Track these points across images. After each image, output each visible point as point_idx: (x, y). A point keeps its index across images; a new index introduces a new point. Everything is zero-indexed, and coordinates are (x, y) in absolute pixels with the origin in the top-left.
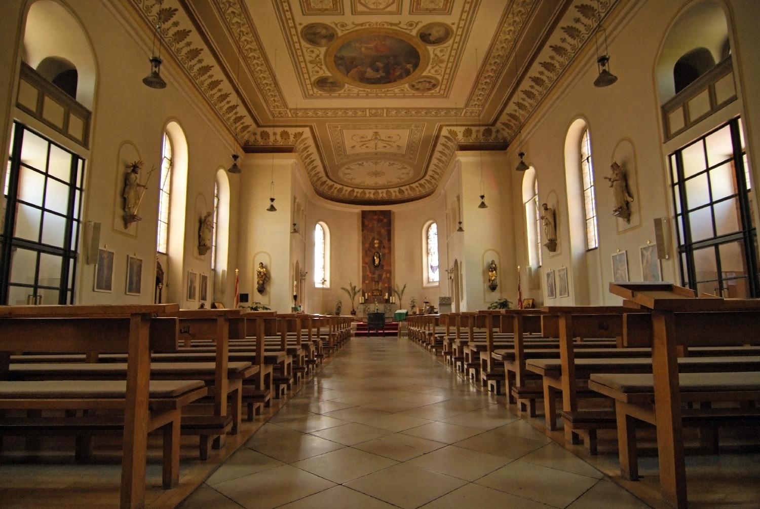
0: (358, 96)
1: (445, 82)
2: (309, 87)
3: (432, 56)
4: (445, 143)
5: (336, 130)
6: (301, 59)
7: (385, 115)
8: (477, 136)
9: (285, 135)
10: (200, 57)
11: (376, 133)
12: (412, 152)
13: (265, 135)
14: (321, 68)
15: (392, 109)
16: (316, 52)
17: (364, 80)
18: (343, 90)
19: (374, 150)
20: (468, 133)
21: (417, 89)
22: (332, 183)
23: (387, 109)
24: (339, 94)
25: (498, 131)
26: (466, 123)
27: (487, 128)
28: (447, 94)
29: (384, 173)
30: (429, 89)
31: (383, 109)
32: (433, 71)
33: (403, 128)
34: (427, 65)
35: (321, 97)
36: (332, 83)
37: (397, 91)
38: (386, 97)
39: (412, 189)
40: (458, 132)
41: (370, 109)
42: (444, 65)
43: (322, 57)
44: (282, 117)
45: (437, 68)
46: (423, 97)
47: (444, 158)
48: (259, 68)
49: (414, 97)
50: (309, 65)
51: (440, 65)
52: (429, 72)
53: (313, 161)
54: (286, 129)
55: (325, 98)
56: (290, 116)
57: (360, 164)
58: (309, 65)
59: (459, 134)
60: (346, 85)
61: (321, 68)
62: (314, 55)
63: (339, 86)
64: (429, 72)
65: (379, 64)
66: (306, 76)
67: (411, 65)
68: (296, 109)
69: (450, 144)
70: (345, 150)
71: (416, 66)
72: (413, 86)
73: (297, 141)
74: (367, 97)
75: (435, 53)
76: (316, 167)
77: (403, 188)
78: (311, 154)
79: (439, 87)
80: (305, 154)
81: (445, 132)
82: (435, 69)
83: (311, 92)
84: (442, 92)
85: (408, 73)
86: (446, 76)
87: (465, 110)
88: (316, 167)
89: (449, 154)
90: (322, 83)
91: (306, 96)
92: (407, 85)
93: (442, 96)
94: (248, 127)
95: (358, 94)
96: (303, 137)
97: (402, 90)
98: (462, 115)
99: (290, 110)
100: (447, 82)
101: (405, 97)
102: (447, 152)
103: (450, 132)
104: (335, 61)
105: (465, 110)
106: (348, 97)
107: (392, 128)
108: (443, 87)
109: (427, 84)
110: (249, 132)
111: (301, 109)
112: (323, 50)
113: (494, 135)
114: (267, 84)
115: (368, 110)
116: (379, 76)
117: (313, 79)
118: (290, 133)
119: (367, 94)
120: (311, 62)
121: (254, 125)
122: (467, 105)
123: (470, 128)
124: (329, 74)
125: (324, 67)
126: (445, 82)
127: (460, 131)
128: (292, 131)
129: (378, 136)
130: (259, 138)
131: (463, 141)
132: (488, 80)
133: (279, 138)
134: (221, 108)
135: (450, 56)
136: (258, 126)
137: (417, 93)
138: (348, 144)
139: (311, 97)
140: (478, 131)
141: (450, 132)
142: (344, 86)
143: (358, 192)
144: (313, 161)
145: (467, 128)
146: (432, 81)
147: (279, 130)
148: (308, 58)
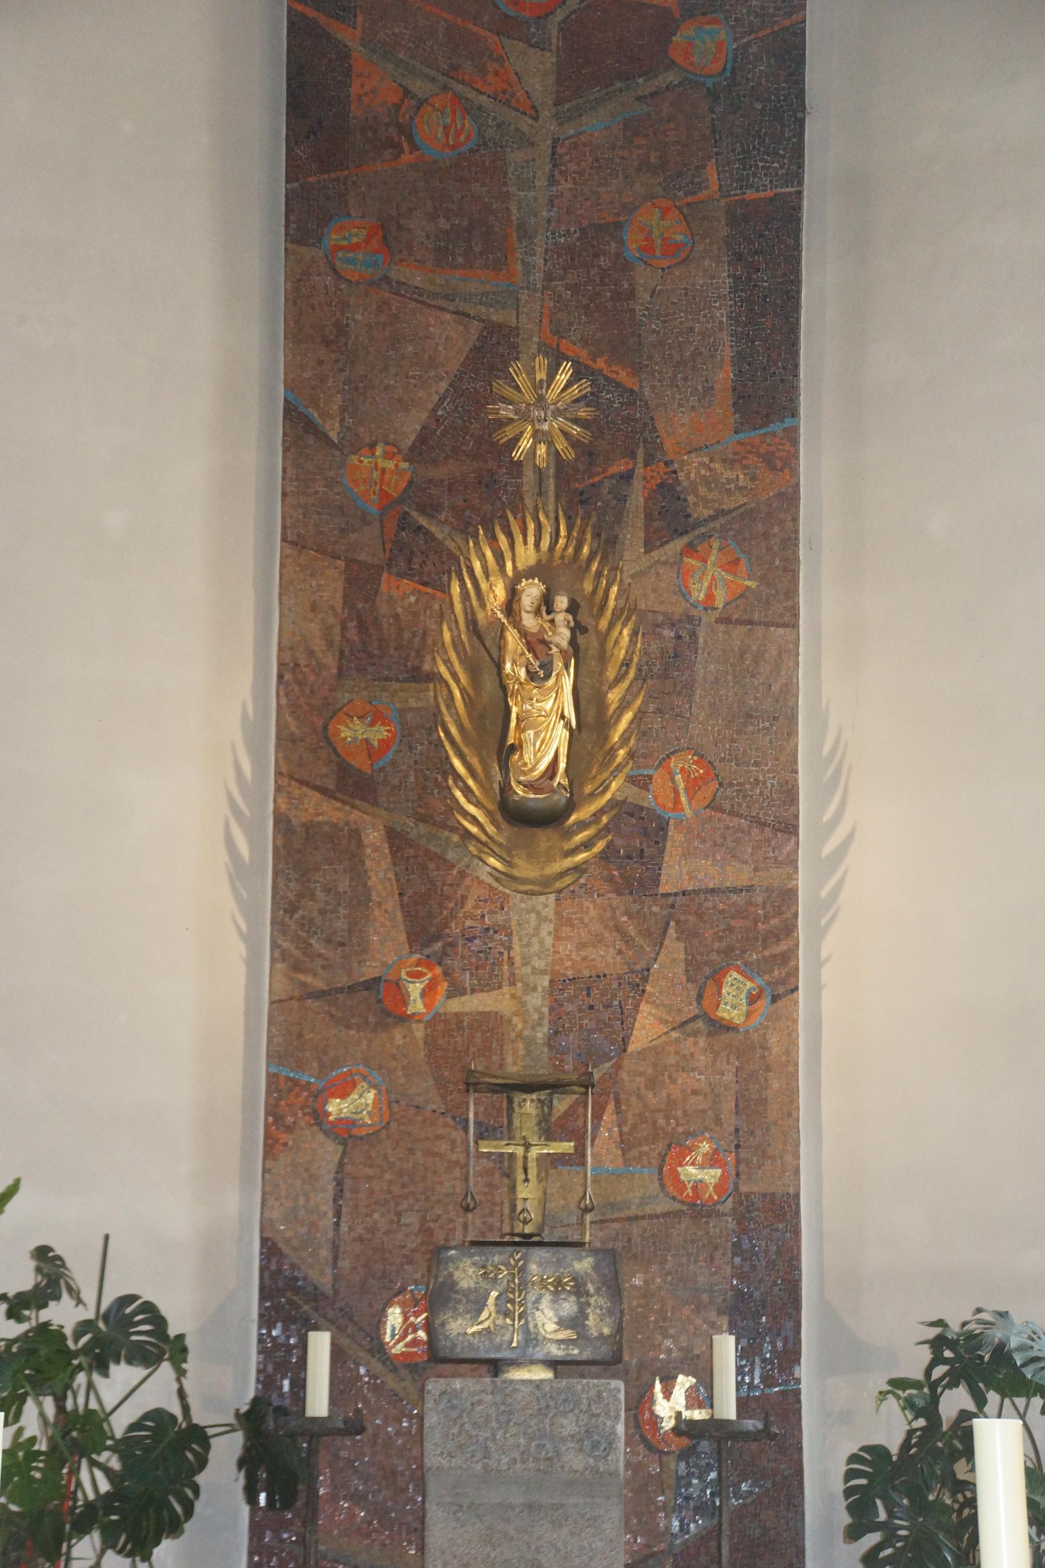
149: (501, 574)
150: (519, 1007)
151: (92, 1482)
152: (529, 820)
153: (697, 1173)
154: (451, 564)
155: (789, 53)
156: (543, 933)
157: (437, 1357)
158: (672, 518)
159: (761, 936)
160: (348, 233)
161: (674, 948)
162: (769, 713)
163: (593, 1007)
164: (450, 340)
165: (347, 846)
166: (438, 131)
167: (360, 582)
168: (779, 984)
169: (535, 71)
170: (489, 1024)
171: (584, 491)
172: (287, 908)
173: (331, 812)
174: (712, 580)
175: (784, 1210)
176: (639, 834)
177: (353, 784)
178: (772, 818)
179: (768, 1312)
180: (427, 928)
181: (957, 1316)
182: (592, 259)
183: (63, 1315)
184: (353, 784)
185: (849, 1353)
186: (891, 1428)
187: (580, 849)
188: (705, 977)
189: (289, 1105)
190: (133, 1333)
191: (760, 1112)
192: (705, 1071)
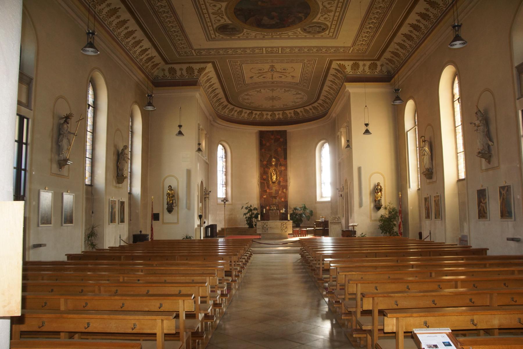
0: (255, 38)
1: (333, 27)
2: (212, 32)
3: (321, 7)
4: (335, 74)
5: (236, 65)
6: (205, 11)
7: (280, 52)
8: (364, 70)
9: (190, 70)
10: (118, 14)
11: (272, 67)
12: (305, 81)
13: (172, 71)
14: (222, 18)
15: (286, 47)
16: (219, 6)
17: (260, 25)
18: (242, 34)
19: (271, 80)
21: (309, 32)
22: (233, 107)
23: (282, 48)
24: (239, 37)
25: (382, 65)
26: (354, 58)
27: (372, 62)
28: (336, 35)
29: (280, 99)
30: (319, 32)
31: (278, 48)
32: (322, 18)
33: (296, 62)
34: (317, 14)
35: (222, 39)
36: (232, 29)
37: (290, 34)
38: (281, 38)
39: (306, 111)
41: (266, 48)
42: (332, 14)
43: (223, 9)
44: (187, 56)
45: (326, 16)
46: (314, 38)
47: (334, 86)
48: (168, 19)
49: (306, 38)
50: (211, 15)
51: (329, 14)
52: (319, 18)
53: (216, 89)
54: (191, 65)
55: (227, 40)
56: (195, 54)
57: (258, 91)
58: (212, 17)
59: (347, 67)
60: (245, 30)
61: (222, 18)
62: (216, 8)
63: (237, 31)
64: (319, 19)
65: (274, 14)
66: (209, 24)
67: (303, 14)
68: (200, 49)
69: (339, 75)
70: (244, 80)
71: (307, 15)
72: (305, 30)
73: (200, 74)
74: (263, 38)
75: (324, 4)
76: (218, 94)
77: (298, 110)
78: (213, 84)
79: (328, 30)
80: (208, 84)
81: (334, 65)
82: (324, 16)
83: (213, 36)
84: (331, 34)
85: (300, 20)
86: (334, 23)
87: (352, 48)
88: (218, 94)
89: (339, 84)
90: (224, 29)
91: (209, 38)
92: (299, 29)
93: (331, 38)
94: (157, 64)
95: (255, 37)
96: (206, 71)
97: (295, 33)
98: (350, 52)
99: (195, 50)
100: (336, 27)
101: (297, 38)
102: (337, 81)
103: (339, 65)
104: (235, 13)
105: (352, 48)
106: (247, 39)
107: (287, 63)
108: (332, 30)
109: (318, 29)
110: (158, 69)
111: (204, 50)
112: (224, 4)
113: (379, 68)
114: (175, 31)
115: (264, 49)
116: (274, 23)
117: (215, 26)
119: (264, 37)
120: (213, 13)
121: (163, 63)
122: (354, 43)
123: (357, 62)
124: (230, 22)
125: (225, 17)
126: (333, 27)
127: (348, 65)
128: (196, 67)
129: (274, 69)
130: (167, 73)
131: (351, 73)
132: (371, 26)
133: (185, 73)
134: (135, 52)
135: (337, 7)
136: (166, 63)
137: (308, 36)
138: (247, 76)
139: (213, 39)
140: (364, 65)
142: (243, 31)
143: (256, 114)
144: (216, 89)
145: (354, 62)
146: (322, 26)
147: (185, 66)
148: (211, 11)
149: (272, 170)
150: (273, 191)
151: (253, 216)
152: (274, 183)
153: (283, 200)
154: (269, 169)
155: (286, 140)
156: (274, 188)
157: (270, 210)
158: (281, 165)
159: (286, 187)
160: (263, 150)
161: (281, 188)
162: (286, 175)
163: (277, 192)
164: (269, 156)
165: (264, 183)
166: (268, 144)
167: (264, 169)
168: (287, 190)
169: (273, 141)
171: (276, 165)
172: (261, 186)
174: (283, 168)
175: (287, 201)
176: (279, 183)
178: (286, 181)
179: (286, 207)
180: (268, 187)
183: (252, 208)
184: (264, 180)
185: (290, 208)
186: (292, 212)
187: (276, 184)
188: (283, 189)
189: (261, 197)
190: (255, 209)
191: (286, 196)
192: (283, 194)
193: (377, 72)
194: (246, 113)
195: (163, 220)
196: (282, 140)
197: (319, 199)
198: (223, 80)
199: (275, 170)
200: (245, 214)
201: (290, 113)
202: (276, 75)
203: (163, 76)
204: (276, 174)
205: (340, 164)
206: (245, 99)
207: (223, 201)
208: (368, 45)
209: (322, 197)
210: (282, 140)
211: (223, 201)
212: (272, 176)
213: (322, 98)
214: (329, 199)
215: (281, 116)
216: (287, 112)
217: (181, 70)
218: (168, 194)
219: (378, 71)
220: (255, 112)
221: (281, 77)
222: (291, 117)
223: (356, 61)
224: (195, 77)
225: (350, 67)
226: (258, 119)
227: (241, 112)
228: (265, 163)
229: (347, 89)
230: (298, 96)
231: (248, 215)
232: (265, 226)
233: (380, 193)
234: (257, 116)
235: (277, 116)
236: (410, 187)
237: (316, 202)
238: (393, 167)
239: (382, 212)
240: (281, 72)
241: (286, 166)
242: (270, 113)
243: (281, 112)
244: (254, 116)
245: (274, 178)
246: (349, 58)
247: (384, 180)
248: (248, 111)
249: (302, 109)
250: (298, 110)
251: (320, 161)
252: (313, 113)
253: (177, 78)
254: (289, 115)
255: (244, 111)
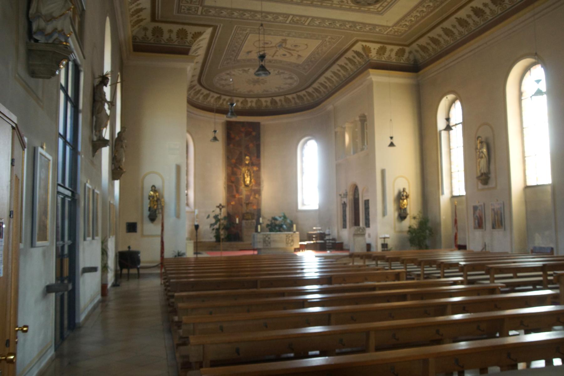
9: (182, 34)
13: (158, 32)
20: (381, 51)
25: (410, 52)
27: (401, 47)
40: (372, 49)
54: (186, 27)
73: (195, 41)
81: (358, 47)
103: (364, 48)
113: (406, 55)
118: (188, 32)
127: (375, 47)
128: (191, 30)
130: (149, 34)
131: (375, 58)
133: (174, 36)
140: (392, 50)
141: (364, 48)
147: (176, 28)
150: (243, 196)
152: (247, 186)
156: (244, 192)
159: (258, 192)
160: (231, 146)
161: (253, 193)
163: (248, 197)
169: (243, 135)
170: (241, 198)
173: (231, 184)
174: (255, 169)
177: (232, 182)
180: (238, 191)
181: (273, 216)
182: (247, 147)
184: (232, 182)
188: (255, 194)
191: (259, 203)
193: (403, 61)
194: (213, 97)
195: (142, 230)
196: (254, 133)
197: (300, 207)
198: (212, 51)
199: (249, 170)
200: (212, 225)
201: (266, 101)
202: (282, 51)
203: (143, 38)
204: (250, 175)
205: (338, 166)
206: (222, 79)
207: (218, 207)
208: (411, 26)
209: (303, 204)
210: (254, 133)
211: (218, 207)
212: (244, 178)
213: (316, 85)
214: (316, 207)
215: (254, 105)
216: (263, 100)
217: (169, 31)
218: (150, 197)
219: (404, 58)
220: (223, 97)
221: (284, 55)
222: (266, 106)
223: (384, 44)
224: (187, 44)
225: (376, 50)
226: (226, 105)
227: (207, 95)
228: (234, 161)
229: (371, 76)
230: (289, 81)
231: (216, 226)
232: (267, 239)
233: (405, 201)
234: (225, 103)
235: (249, 104)
236: (443, 193)
237: (298, 211)
238: (418, 171)
239: (408, 222)
240: (290, 49)
241: (259, 165)
242: (241, 100)
243: (254, 100)
244: (221, 101)
245: (248, 180)
246: (377, 40)
247: (409, 186)
248: (216, 96)
249: (282, 98)
250: (277, 99)
251: (302, 161)
252: (296, 103)
253: (163, 42)
254: (264, 104)
255: (212, 94)
